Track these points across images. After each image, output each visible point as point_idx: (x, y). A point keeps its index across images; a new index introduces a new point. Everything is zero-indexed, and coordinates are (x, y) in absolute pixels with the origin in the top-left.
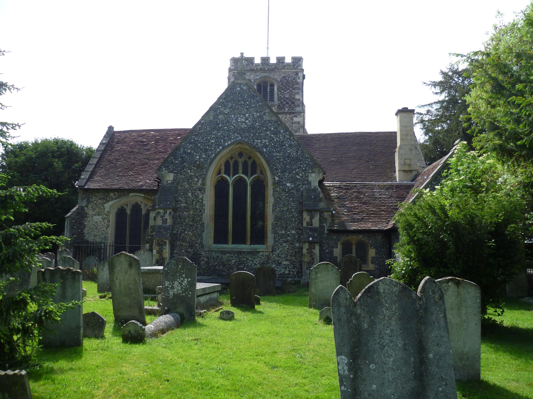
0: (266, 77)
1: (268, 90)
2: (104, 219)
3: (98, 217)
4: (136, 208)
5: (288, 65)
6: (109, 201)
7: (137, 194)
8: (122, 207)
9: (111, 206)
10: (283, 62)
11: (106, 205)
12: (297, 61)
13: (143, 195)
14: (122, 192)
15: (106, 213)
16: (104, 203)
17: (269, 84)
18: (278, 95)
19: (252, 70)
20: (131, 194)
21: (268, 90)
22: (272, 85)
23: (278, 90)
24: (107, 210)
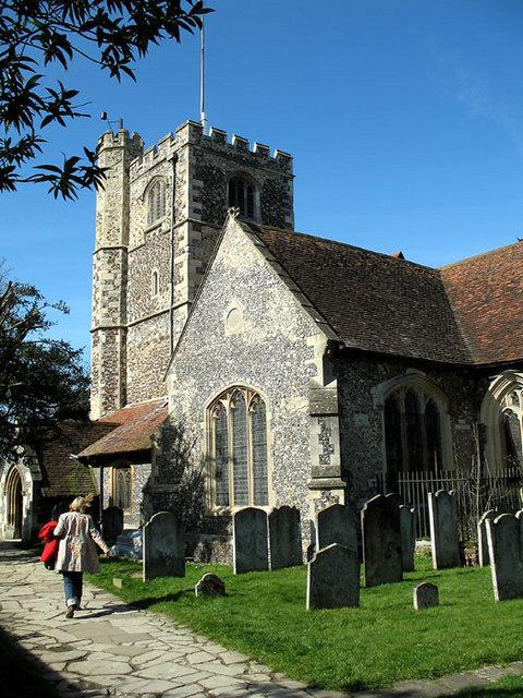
0: (243, 172)
1: (245, 196)
2: (372, 421)
3: (362, 416)
4: (411, 397)
5: (273, 161)
6: (379, 382)
7: (416, 371)
8: (392, 396)
9: (379, 393)
10: (266, 155)
11: (373, 390)
12: (285, 160)
13: (424, 374)
14: (400, 363)
15: (375, 407)
16: (371, 387)
17: (246, 186)
18: (262, 209)
19: (223, 154)
20: (409, 371)
21: (245, 196)
22: (251, 190)
23: (261, 200)
24: (375, 401)
